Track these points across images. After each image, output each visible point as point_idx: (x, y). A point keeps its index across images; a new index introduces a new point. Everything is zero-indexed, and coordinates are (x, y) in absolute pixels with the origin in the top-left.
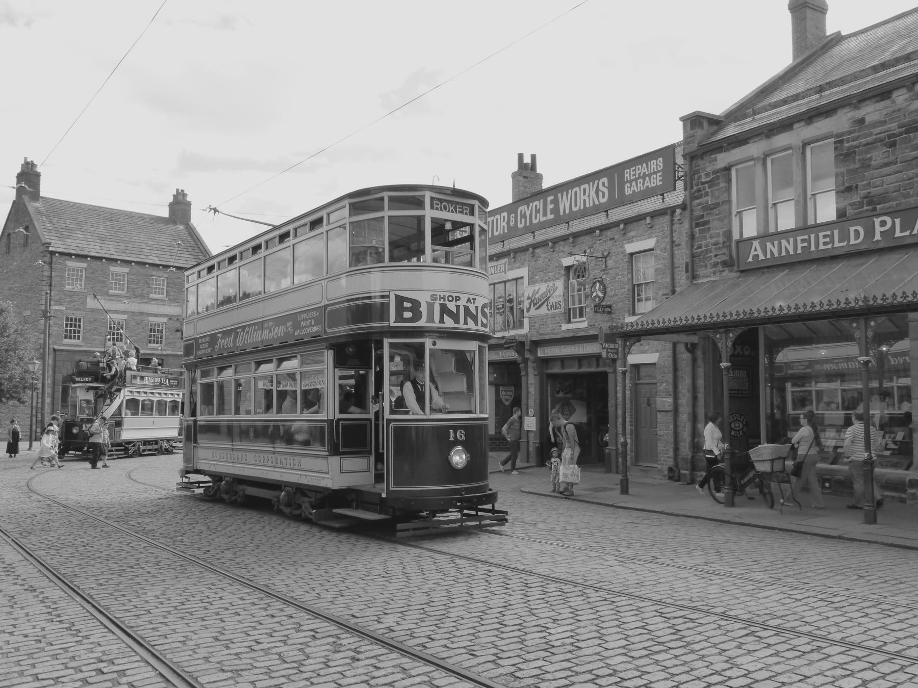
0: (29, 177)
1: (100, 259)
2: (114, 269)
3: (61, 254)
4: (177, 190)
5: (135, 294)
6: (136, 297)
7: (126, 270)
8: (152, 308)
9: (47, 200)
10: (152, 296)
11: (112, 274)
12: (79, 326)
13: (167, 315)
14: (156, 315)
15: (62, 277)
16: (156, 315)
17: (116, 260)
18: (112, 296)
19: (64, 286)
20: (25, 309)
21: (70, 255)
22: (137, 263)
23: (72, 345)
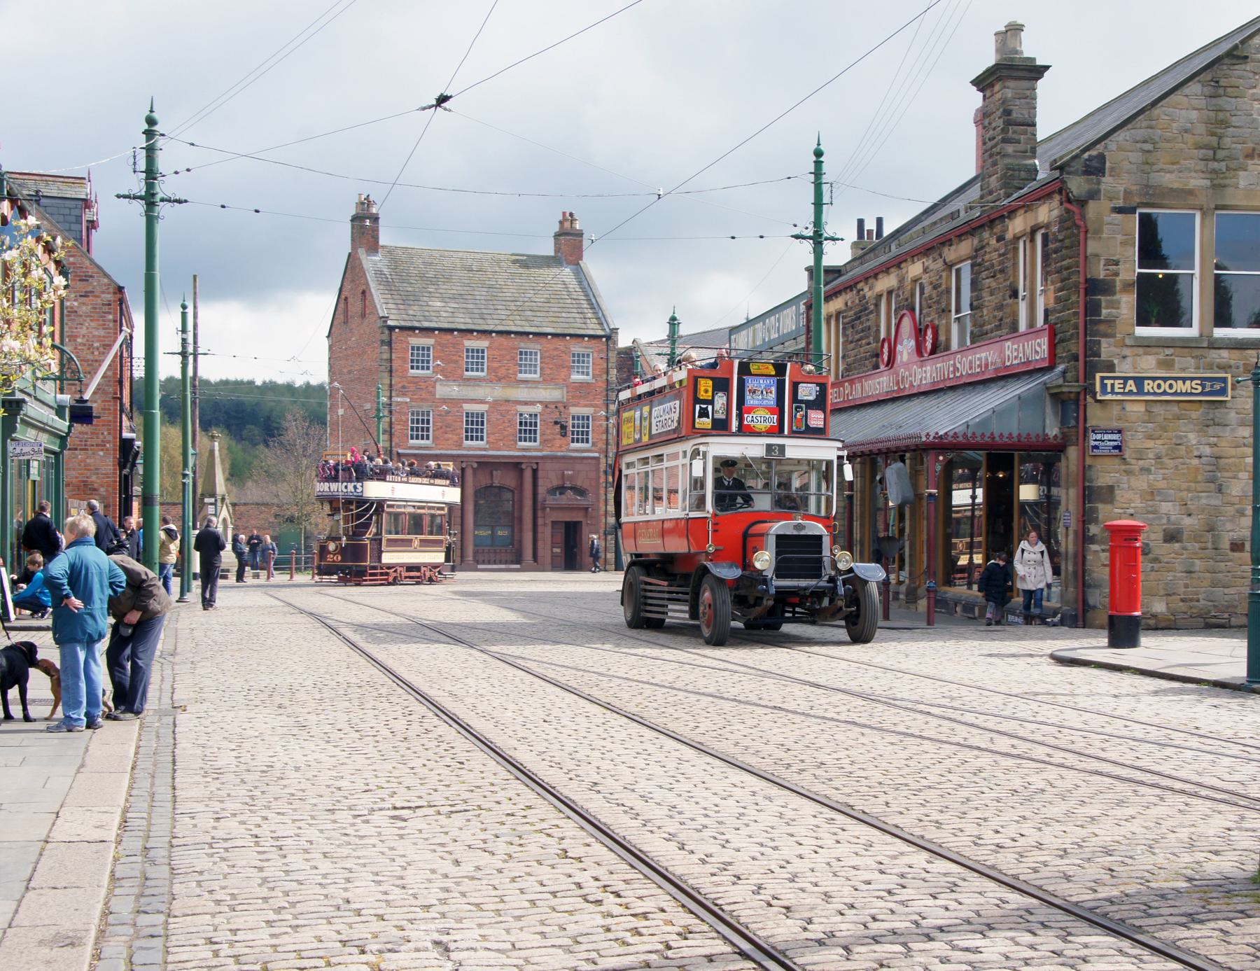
0: (365, 225)
1: (451, 331)
2: (470, 343)
3: (401, 328)
4: (564, 213)
5: (497, 377)
6: (499, 380)
7: (483, 343)
8: (521, 393)
9: (390, 251)
10: (521, 376)
11: (468, 351)
12: (428, 422)
13: (540, 402)
14: (526, 403)
15: (404, 359)
16: (526, 403)
17: (471, 331)
18: (469, 379)
19: (407, 371)
20: (367, 401)
21: (412, 329)
22: (500, 333)
23: (420, 448)
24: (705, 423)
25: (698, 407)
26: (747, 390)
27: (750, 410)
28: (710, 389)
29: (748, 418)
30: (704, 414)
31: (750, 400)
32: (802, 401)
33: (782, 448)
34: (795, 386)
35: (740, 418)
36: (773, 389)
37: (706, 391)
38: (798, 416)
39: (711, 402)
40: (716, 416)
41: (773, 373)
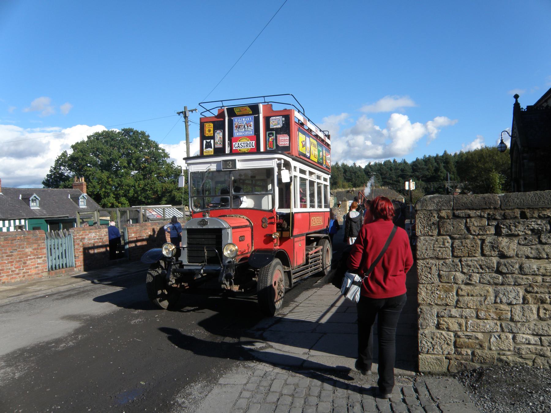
24: (211, 151)
25: (205, 142)
26: (234, 126)
27: (237, 139)
28: (212, 129)
29: (235, 145)
30: (209, 146)
31: (236, 133)
32: (273, 129)
33: (234, 161)
34: (267, 120)
35: (231, 145)
36: (252, 123)
37: (209, 131)
38: (270, 140)
39: (213, 138)
40: (216, 146)
41: (251, 112)
